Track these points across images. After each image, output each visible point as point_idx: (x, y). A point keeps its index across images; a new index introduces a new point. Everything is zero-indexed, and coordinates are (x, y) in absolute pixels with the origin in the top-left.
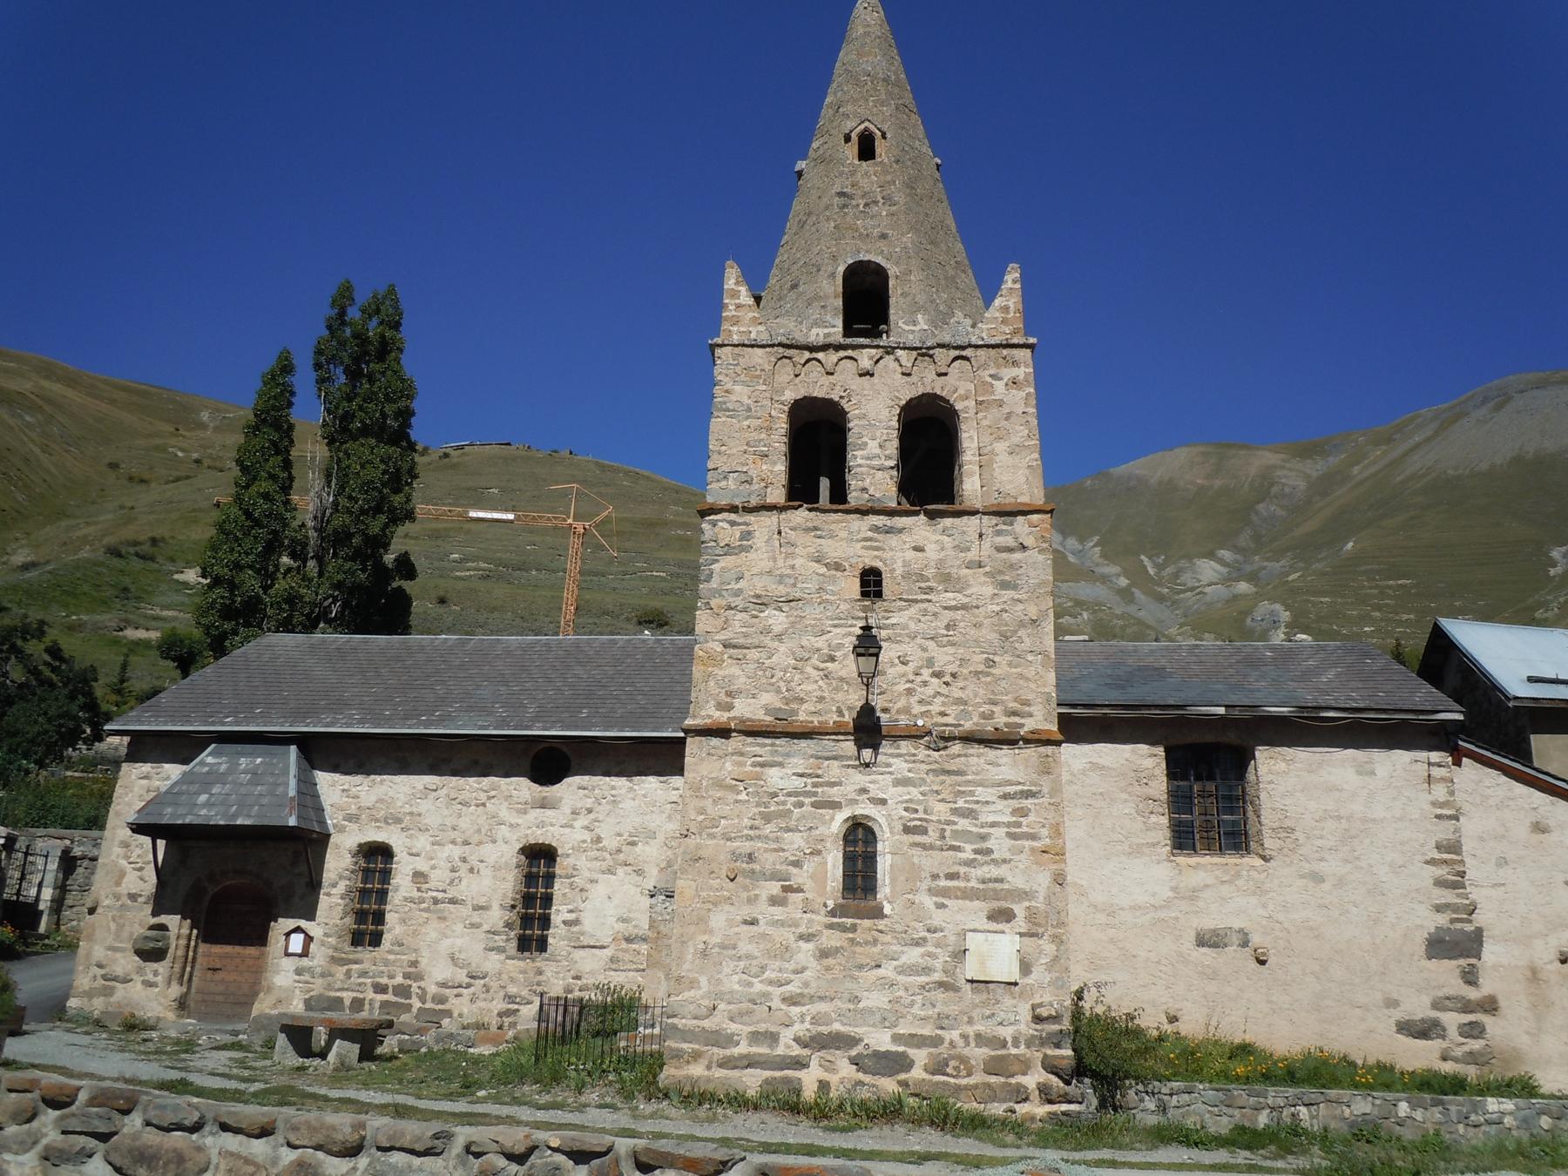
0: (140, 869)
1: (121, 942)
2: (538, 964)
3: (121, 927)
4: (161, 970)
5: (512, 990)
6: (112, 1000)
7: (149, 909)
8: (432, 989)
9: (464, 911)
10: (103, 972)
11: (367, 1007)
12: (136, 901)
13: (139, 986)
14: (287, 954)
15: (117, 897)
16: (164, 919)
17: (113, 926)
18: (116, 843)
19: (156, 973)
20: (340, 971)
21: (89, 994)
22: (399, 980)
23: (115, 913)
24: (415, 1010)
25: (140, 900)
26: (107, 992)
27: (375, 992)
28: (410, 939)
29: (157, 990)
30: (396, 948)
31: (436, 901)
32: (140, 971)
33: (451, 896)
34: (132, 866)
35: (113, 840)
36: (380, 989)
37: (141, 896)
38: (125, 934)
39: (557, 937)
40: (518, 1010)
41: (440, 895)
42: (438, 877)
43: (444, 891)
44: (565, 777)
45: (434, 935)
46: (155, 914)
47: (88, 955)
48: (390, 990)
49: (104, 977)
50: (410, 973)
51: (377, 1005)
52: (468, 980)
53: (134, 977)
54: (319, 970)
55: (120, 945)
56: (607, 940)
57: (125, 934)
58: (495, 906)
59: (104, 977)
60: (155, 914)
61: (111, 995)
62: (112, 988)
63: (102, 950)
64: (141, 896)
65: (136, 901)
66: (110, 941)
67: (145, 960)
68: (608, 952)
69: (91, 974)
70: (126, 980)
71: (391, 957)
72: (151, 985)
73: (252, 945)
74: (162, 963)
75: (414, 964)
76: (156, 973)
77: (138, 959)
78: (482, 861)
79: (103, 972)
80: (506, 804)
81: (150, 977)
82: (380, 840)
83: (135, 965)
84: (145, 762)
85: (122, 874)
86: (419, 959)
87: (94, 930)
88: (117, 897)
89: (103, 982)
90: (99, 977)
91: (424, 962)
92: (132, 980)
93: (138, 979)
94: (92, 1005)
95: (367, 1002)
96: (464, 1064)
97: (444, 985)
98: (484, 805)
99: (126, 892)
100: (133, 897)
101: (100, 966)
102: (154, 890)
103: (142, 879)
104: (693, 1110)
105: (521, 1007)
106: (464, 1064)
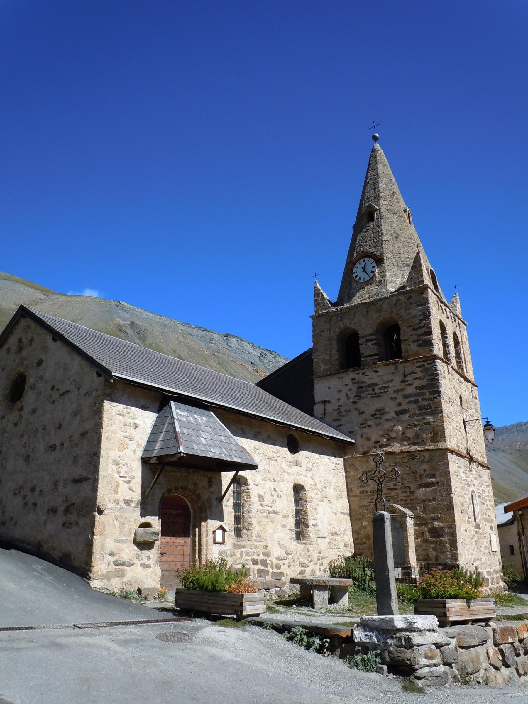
0: (129, 482)
1: (124, 536)
2: (308, 546)
3: (122, 524)
4: (152, 556)
5: (302, 560)
6: (125, 579)
7: (138, 511)
8: (275, 562)
9: (279, 518)
10: (113, 559)
11: (251, 573)
12: (129, 505)
13: (140, 569)
14: (215, 543)
15: (117, 502)
16: (149, 519)
17: (117, 524)
18: (110, 461)
19: (149, 558)
20: (238, 552)
21: (108, 577)
22: (261, 557)
23: (116, 514)
24: (270, 573)
25: (132, 504)
26: (121, 574)
27: (253, 564)
28: (263, 533)
29: (150, 570)
30: (258, 539)
31: (269, 513)
32: (138, 557)
33: (274, 510)
34: (123, 479)
35: (108, 458)
36: (255, 562)
37: (132, 502)
38: (126, 529)
39: (311, 532)
40: (305, 571)
41: (270, 509)
42: (268, 498)
43: (271, 507)
44: (301, 451)
45: (271, 531)
46: (143, 515)
47: (103, 547)
48: (259, 562)
49: (116, 563)
50: (265, 552)
51: (256, 572)
52: (286, 556)
53: (135, 561)
54: (229, 552)
55: (124, 538)
56: (326, 534)
57: (126, 529)
58: (291, 516)
59: (116, 563)
60: (143, 515)
61: (123, 576)
62: (122, 571)
63: (112, 542)
64: (132, 502)
65: (129, 505)
66: (117, 535)
67: (141, 549)
68: (327, 540)
69: (106, 561)
70: (131, 565)
71: (257, 543)
72: (148, 567)
73: (180, 536)
74: (152, 551)
75: (266, 547)
76: (149, 558)
77: (136, 548)
78: (281, 491)
79: (113, 559)
80: (284, 461)
81: (145, 561)
82: (242, 475)
83: (135, 553)
84: (119, 403)
85: (117, 485)
86: (268, 544)
87: (104, 527)
88: (117, 502)
89: (115, 567)
90: (112, 563)
91: (270, 546)
92: (134, 564)
93: (138, 562)
94: (112, 585)
95: (251, 570)
96: (462, 582)
97: (278, 559)
98: (276, 460)
99: (122, 498)
100: (127, 502)
101: (111, 554)
102: (140, 498)
103: (131, 490)
104: (263, 628)
105: (306, 569)
106: (462, 582)
